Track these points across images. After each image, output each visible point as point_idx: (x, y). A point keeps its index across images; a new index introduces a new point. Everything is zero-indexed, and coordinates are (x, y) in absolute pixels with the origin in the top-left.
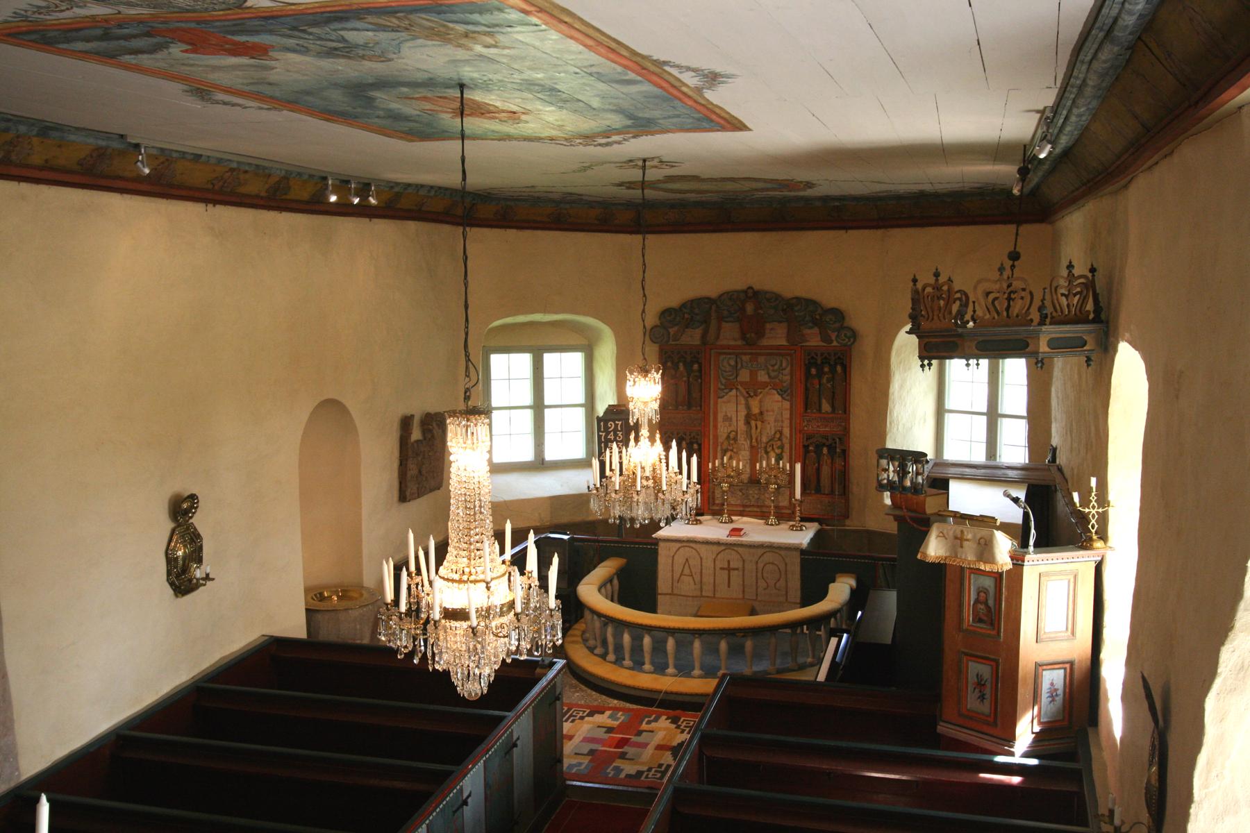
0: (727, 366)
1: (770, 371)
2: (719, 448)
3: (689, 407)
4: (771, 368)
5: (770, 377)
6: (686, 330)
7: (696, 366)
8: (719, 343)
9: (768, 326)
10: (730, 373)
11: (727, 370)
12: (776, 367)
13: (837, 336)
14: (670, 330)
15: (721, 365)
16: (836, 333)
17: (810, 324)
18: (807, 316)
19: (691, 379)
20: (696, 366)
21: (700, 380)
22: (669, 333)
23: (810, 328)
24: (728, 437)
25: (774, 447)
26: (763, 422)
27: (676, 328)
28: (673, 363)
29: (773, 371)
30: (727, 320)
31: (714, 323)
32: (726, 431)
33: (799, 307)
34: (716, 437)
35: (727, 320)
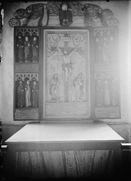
0: (52, 40)
1: (75, 42)
2: (48, 84)
3: (31, 61)
4: (75, 40)
5: (75, 45)
6: (30, 20)
7: (35, 39)
8: (48, 26)
9: (74, 17)
10: (54, 44)
11: (52, 42)
12: (78, 40)
13: (110, 22)
14: (21, 20)
15: (48, 39)
16: (109, 21)
17: (96, 17)
18: (94, 13)
19: (32, 46)
20: (35, 39)
21: (37, 46)
22: (20, 22)
23: (97, 19)
24: (54, 78)
25: (80, 81)
26: (72, 68)
27: (24, 19)
28: (22, 36)
29: (77, 42)
30: (52, 15)
31: (45, 15)
32: (52, 74)
33: (90, 8)
34: (46, 79)
35: (52, 15)
